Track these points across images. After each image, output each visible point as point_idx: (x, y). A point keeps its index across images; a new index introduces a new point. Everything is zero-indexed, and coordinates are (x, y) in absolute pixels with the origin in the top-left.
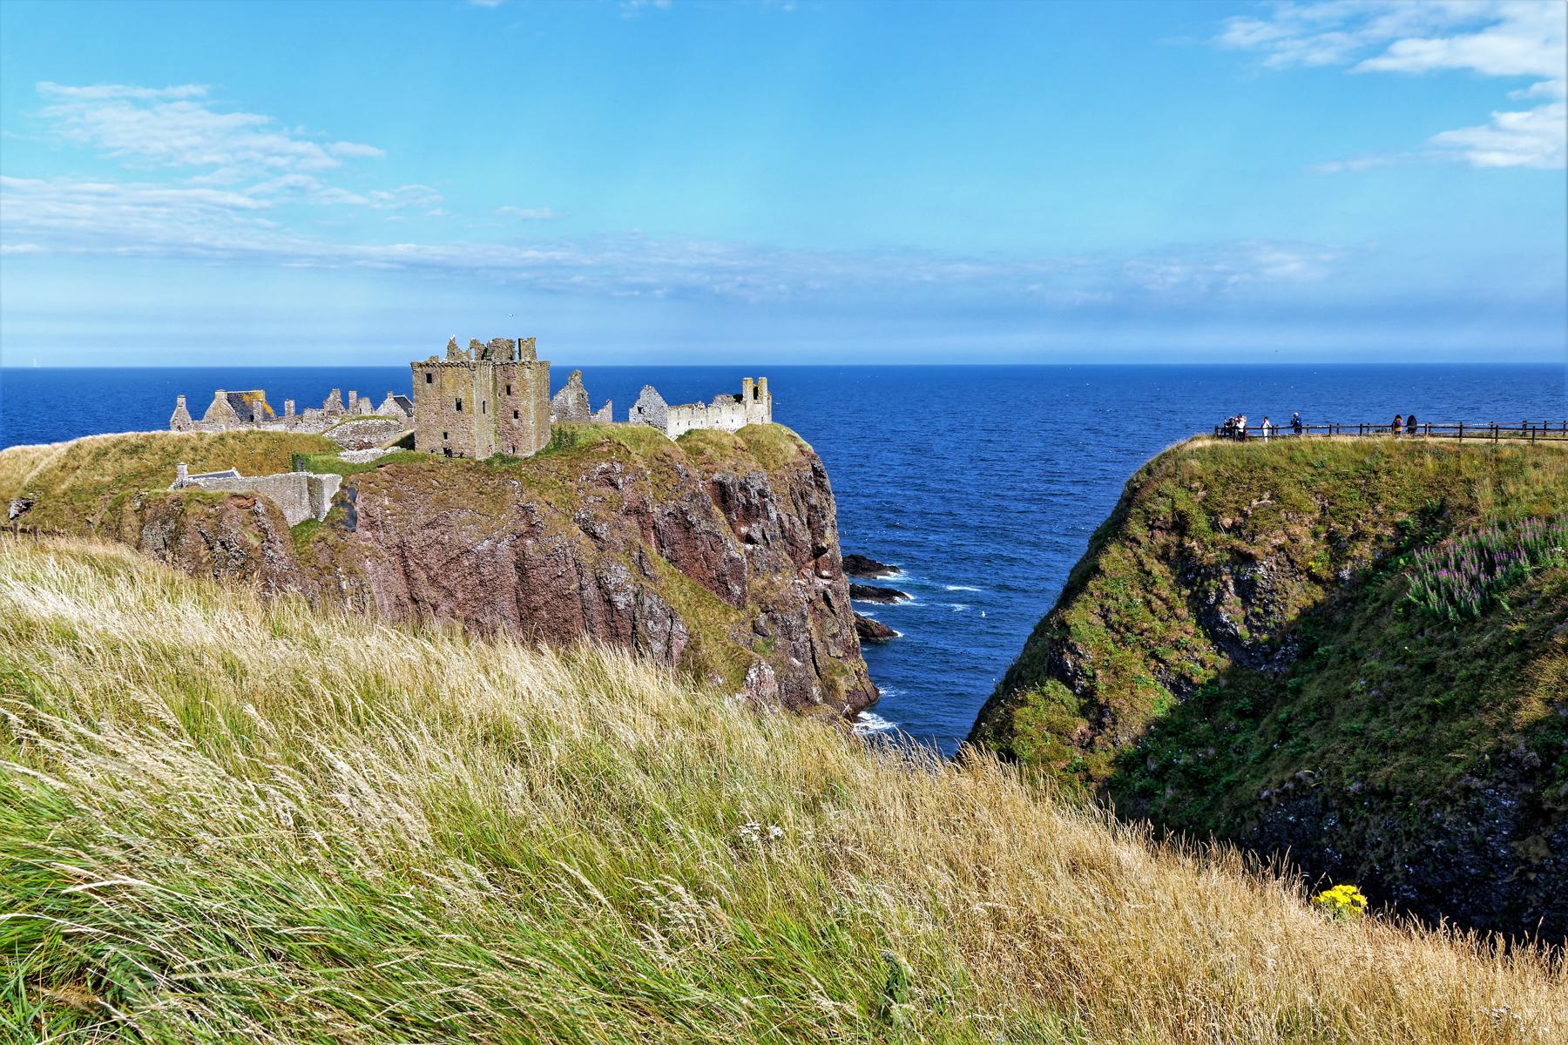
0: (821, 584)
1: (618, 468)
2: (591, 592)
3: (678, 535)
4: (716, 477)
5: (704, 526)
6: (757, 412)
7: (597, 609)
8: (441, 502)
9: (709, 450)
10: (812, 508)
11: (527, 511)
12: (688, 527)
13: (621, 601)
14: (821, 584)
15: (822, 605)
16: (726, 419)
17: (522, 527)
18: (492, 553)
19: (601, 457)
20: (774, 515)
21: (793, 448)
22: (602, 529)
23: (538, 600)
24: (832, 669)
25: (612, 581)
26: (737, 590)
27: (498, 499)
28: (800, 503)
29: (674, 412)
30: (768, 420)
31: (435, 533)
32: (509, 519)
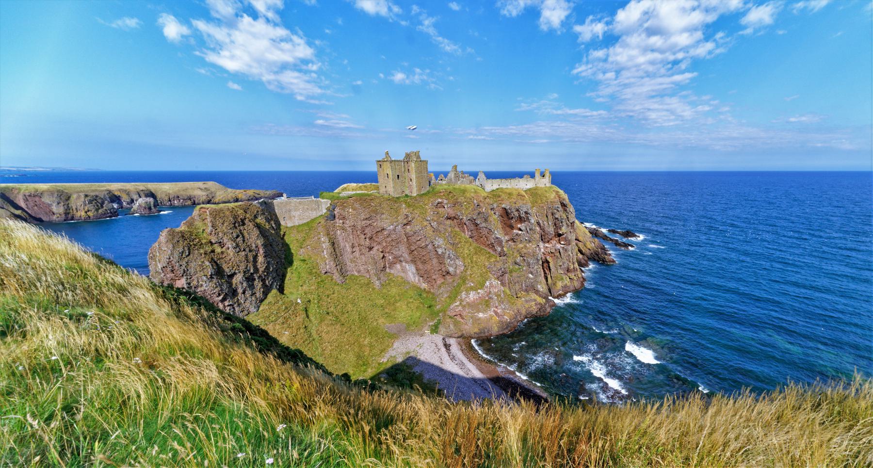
0: (559, 246)
1: (445, 201)
2: (430, 247)
3: (473, 227)
4: (503, 206)
5: (484, 225)
6: (545, 183)
7: (433, 254)
8: (373, 211)
9: (503, 196)
10: (557, 219)
11: (407, 216)
12: (477, 225)
13: (440, 251)
14: (559, 246)
15: (558, 254)
16: (525, 184)
17: (405, 222)
18: (394, 230)
19: (440, 197)
20: (533, 221)
21: (553, 195)
22: (434, 224)
23: (413, 248)
24: (557, 278)
25: (436, 243)
26: (499, 249)
27: (397, 211)
28: (550, 217)
29: (490, 181)
30: (548, 185)
31: (368, 222)
32: (401, 219)
